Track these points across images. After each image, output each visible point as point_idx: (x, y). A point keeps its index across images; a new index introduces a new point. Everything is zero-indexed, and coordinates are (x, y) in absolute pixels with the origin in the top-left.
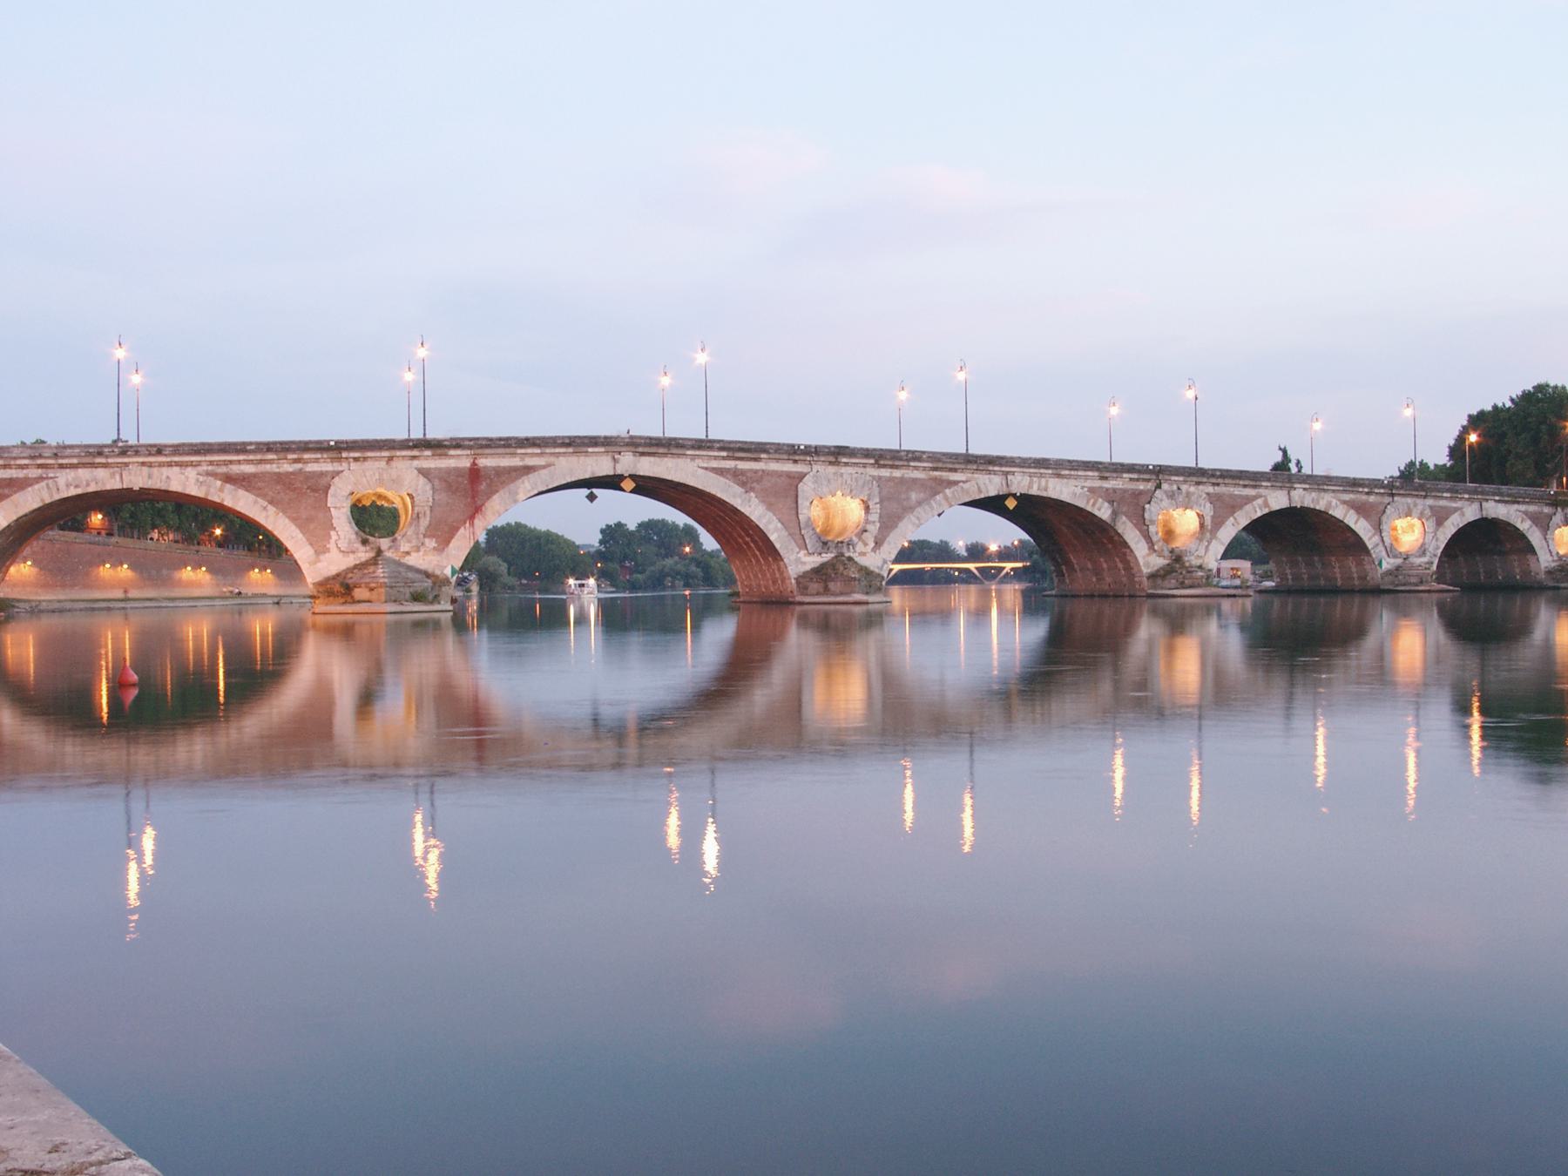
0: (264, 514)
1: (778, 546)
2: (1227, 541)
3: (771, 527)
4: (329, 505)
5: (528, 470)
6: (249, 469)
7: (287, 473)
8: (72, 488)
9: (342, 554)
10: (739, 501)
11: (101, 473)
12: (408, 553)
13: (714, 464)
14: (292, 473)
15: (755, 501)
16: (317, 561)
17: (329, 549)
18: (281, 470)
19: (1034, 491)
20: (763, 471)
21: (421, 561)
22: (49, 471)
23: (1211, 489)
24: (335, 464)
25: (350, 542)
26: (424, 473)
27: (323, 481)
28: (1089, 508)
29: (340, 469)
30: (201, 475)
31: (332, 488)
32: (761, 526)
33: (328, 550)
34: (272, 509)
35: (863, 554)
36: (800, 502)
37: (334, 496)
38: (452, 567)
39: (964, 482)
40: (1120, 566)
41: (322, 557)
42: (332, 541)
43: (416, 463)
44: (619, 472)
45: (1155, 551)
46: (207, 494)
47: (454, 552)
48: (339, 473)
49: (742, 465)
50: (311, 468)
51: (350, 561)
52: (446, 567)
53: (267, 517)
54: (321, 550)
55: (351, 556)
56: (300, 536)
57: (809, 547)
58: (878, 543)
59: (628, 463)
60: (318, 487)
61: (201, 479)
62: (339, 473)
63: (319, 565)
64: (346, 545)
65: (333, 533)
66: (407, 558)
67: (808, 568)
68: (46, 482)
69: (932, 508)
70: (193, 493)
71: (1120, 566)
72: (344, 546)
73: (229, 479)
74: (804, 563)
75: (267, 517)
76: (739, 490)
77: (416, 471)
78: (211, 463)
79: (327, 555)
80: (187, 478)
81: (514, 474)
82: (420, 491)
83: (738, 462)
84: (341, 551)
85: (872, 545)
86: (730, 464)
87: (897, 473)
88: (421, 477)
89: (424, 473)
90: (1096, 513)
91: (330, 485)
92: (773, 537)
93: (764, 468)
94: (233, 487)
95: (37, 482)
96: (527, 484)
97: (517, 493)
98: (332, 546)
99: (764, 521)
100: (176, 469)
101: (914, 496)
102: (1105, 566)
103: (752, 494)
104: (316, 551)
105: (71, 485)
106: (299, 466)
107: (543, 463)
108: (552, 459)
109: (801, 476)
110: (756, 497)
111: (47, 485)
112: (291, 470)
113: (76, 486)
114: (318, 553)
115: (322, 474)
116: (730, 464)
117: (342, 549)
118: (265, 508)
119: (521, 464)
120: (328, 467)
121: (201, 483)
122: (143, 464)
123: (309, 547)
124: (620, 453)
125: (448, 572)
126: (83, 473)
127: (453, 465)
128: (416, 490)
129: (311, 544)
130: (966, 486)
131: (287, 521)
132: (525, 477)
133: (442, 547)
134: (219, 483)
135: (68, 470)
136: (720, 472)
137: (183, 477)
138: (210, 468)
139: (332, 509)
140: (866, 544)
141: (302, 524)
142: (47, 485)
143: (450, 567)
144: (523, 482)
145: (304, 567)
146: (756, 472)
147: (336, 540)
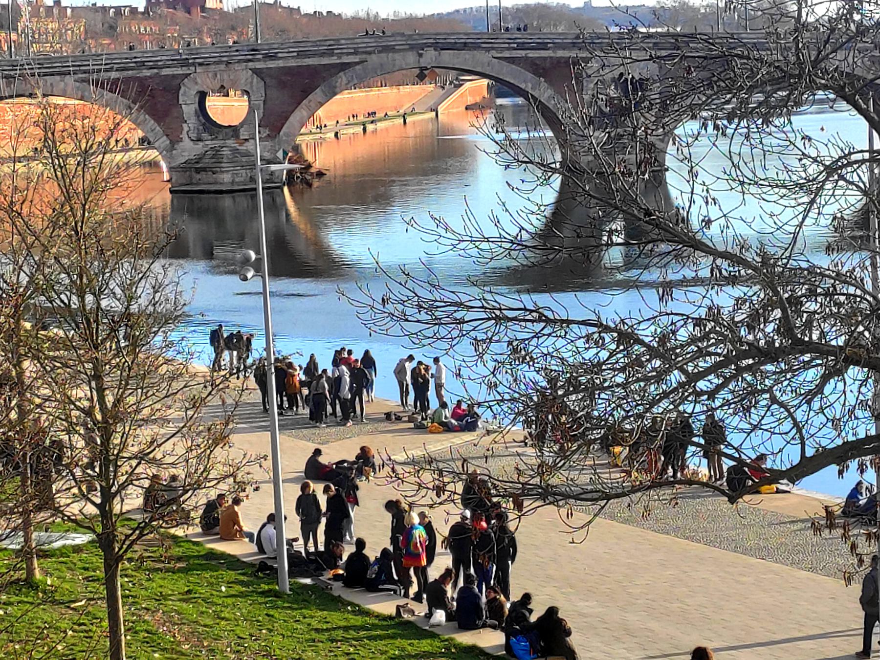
4: (180, 102)
7: (146, 76)
9: (192, 143)
10: (530, 85)
12: (246, 140)
13: (507, 54)
14: (150, 77)
17: (182, 138)
18: (141, 75)
20: (551, 57)
24: (183, 68)
26: (255, 71)
27: (176, 82)
30: (77, 81)
31: (183, 88)
33: (181, 140)
37: (184, 94)
42: (185, 132)
43: (251, 65)
47: (284, 138)
48: (187, 75)
49: (532, 54)
50: (165, 72)
52: (277, 151)
54: (175, 141)
55: (199, 143)
56: (158, 128)
61: (78, 84)
63: (174, 152)
64: (195, 135)
65: (185, 126)
66: (247, 144)
72: (194, 136)
76: (530, 75)
77: (250, 72)
79: (181, 144)
80: (66, 84)
81: (333, 70)
82: (254, 88)
83: (528, 51)
84: (192, 140)
86: (522, 53)
89: (255, 71)
91: (180, 87)
93: (552, 55)
98: (184, 136)
100: (58, 78)
103: (542, 79)
104: (171, 141)
106: (156, 71)
107: (357, 60)
108: (364, 56)
110: (545, 81)
112: (149, 74)
115: (174, 76)
117: (192, 138)
119: (338, 61)
120: (179, 71)
123: (165, 137)
127: (282, 65)
129: (167, 136)
131: (147, 116)
132: (341, 74)
133: (274, 134)
136: (511, 60)
137: (63, 83)
138: (84, 75)
139: (183, 106)
143: (281, 150)
144: (340, 77)
146: (545, 58)
147: (188, 132)
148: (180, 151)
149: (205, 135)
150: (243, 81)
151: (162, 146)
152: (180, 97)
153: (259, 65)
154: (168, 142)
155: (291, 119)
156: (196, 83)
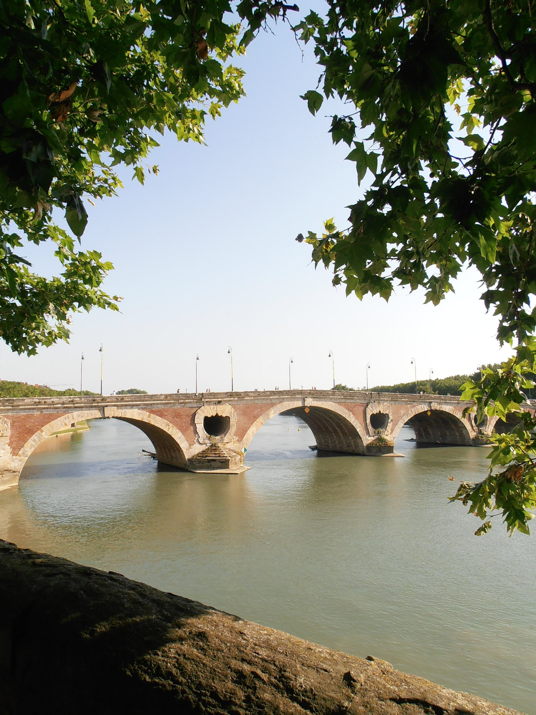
0: (168, 427)
1: (360, 433)
2: (494, 425)
3: (357, 426)
5: (273, 405)
8: (80, 417)
12: (227, 443)
15: (352, 415)
16: (190, 448)
19: (438, 409)
21: (232, 446)
22: (69, 409)
25: (204, 439)
28: (454, 414)
29: (200, 406)
32: (354, 426)
34: (171, 425)
35: (387, 435)
36: (367, 415)
37: (198, 418)
38: (245, 448)
39: (417, 406)
40: (458, 435)
41: (192, 447)
44: (306, 405)
45: (474, 430)
46: (143, 419)
51: (204, 447)
53: (169, 429)
54: (191, 444)
56: (183, 437)
57: (370, 433)
58: (392, 431)
59: (310, 402)
61: (140, 411)
66: (227, 445)
67: (369, 442)
68: (67, 415)
69: (408, 416)
70: (136, 419)
71: (458, 435)
73: (152, 412)
74: (368, 440)
75: (169, 429)
78: (145, 404)
82: (232, 415)
85: (390, 432)
88: (233, 409)
90: (456, 416)
92: (358, 430)
94: (154, 415)
95: (63, 415)
96: (272, 410)
97: (269, 415)
99: (355, 423)
101: (402, 412)
102: (448, 434)
103: (351, 413)
105: (79, 416)
111: (68, 416)
113: (82, 417)
114: (191, 444)
118: (168, 425)
121: (140, 413)
122: (115, 406)
124: (306, 397)
125: (243, 450)
128: (231, 415)
129: (187, 441)
130: (418, 407)
134: (148, 413)
135: (78, 409)
140: (388, 431)
141: (183, 430)
142: (68, 416)
143: (243, 448)
145: (184, 451)
148: (194, 449)
149: (207, 441)
150: (227, 411)
151: (184, 446)
152: (196, 420)
154: (188, 444)
155: (248, 432)
156: (204, 412)
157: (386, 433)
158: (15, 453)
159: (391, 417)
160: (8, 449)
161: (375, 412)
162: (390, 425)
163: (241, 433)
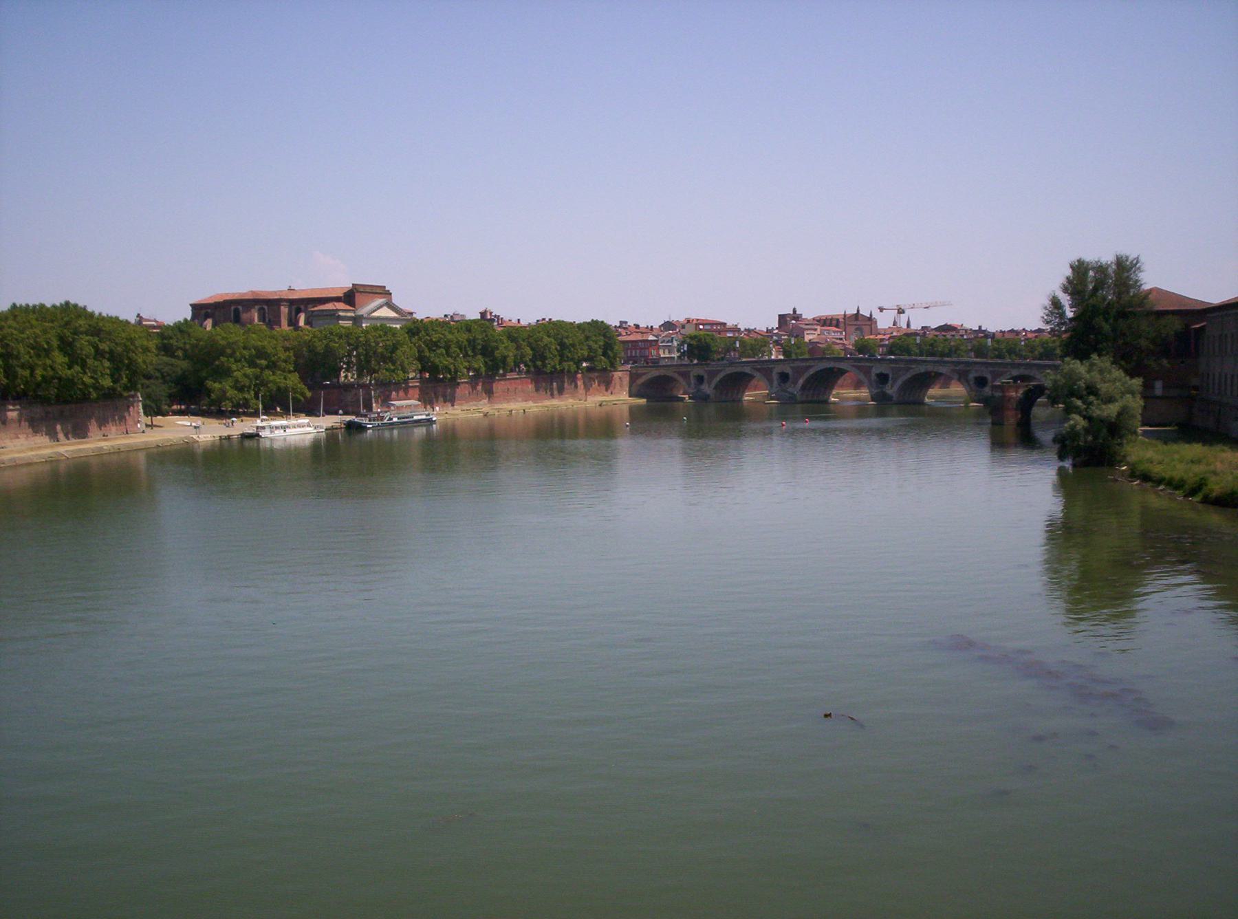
6: (759, 367)
11: (733, 368)
23: (991, 369)
50: (770, 366)
58: (892, 386)
60: (771, 370)
62: (774, 368)
73: (754, 369)
86: (856, 364)
87: (897, 366)
89: (791, 367)
109: (872, 367)
116: (856, 364)
120: (773, 366)
126: (730, 368)
136: (853, 366)
153: (792, 365)
157: (887, 388)
158: (709, 387)
159: (890, 376)
160: (707, 385)
161: (878, 372)
162: (890, 382)
163: (795, 383)
